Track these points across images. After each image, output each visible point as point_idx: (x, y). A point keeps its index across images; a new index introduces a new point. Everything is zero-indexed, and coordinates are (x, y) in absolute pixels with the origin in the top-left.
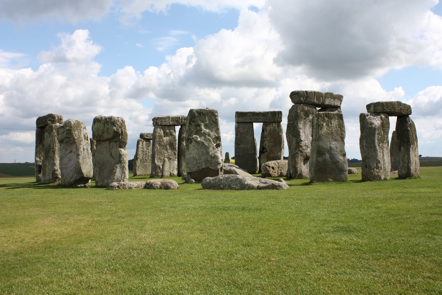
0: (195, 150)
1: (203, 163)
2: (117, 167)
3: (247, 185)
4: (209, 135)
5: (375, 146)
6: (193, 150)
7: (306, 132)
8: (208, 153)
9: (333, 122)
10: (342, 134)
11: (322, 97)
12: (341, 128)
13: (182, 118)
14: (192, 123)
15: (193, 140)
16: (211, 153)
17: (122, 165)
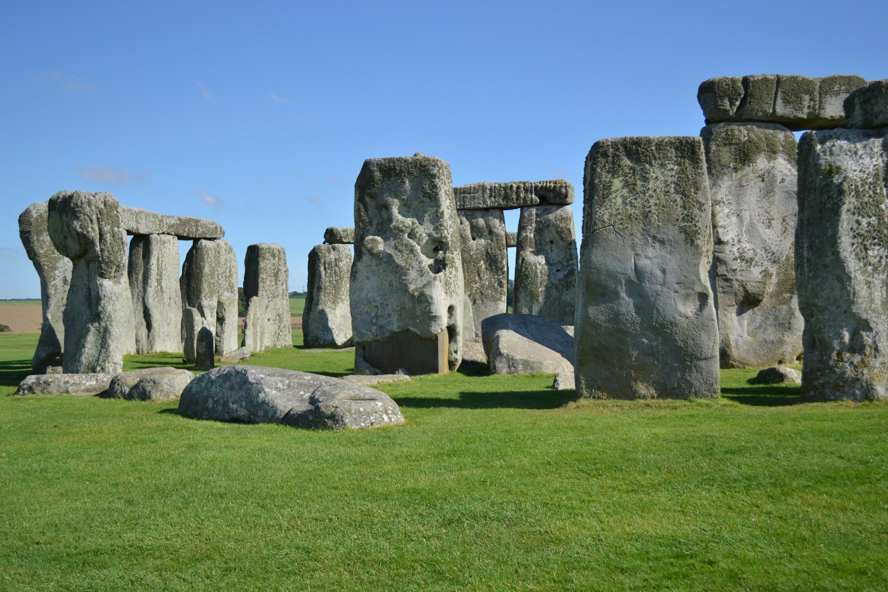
0: (373, 279)
1: (395, 319)
2: (88, 330)
3: (264, 402)
4: (412, 235)
5: (839, 263)
6: (368, 279)
7: (746, 215)
8: (404, 288)
9: (655, 172)
10: (689, 218)
11: (810, 93)
12: (684, 194)
13: (518, 187)
14: (367, 199)
15: (364, 250)
16: (412, 287)
17: (103, 324)
